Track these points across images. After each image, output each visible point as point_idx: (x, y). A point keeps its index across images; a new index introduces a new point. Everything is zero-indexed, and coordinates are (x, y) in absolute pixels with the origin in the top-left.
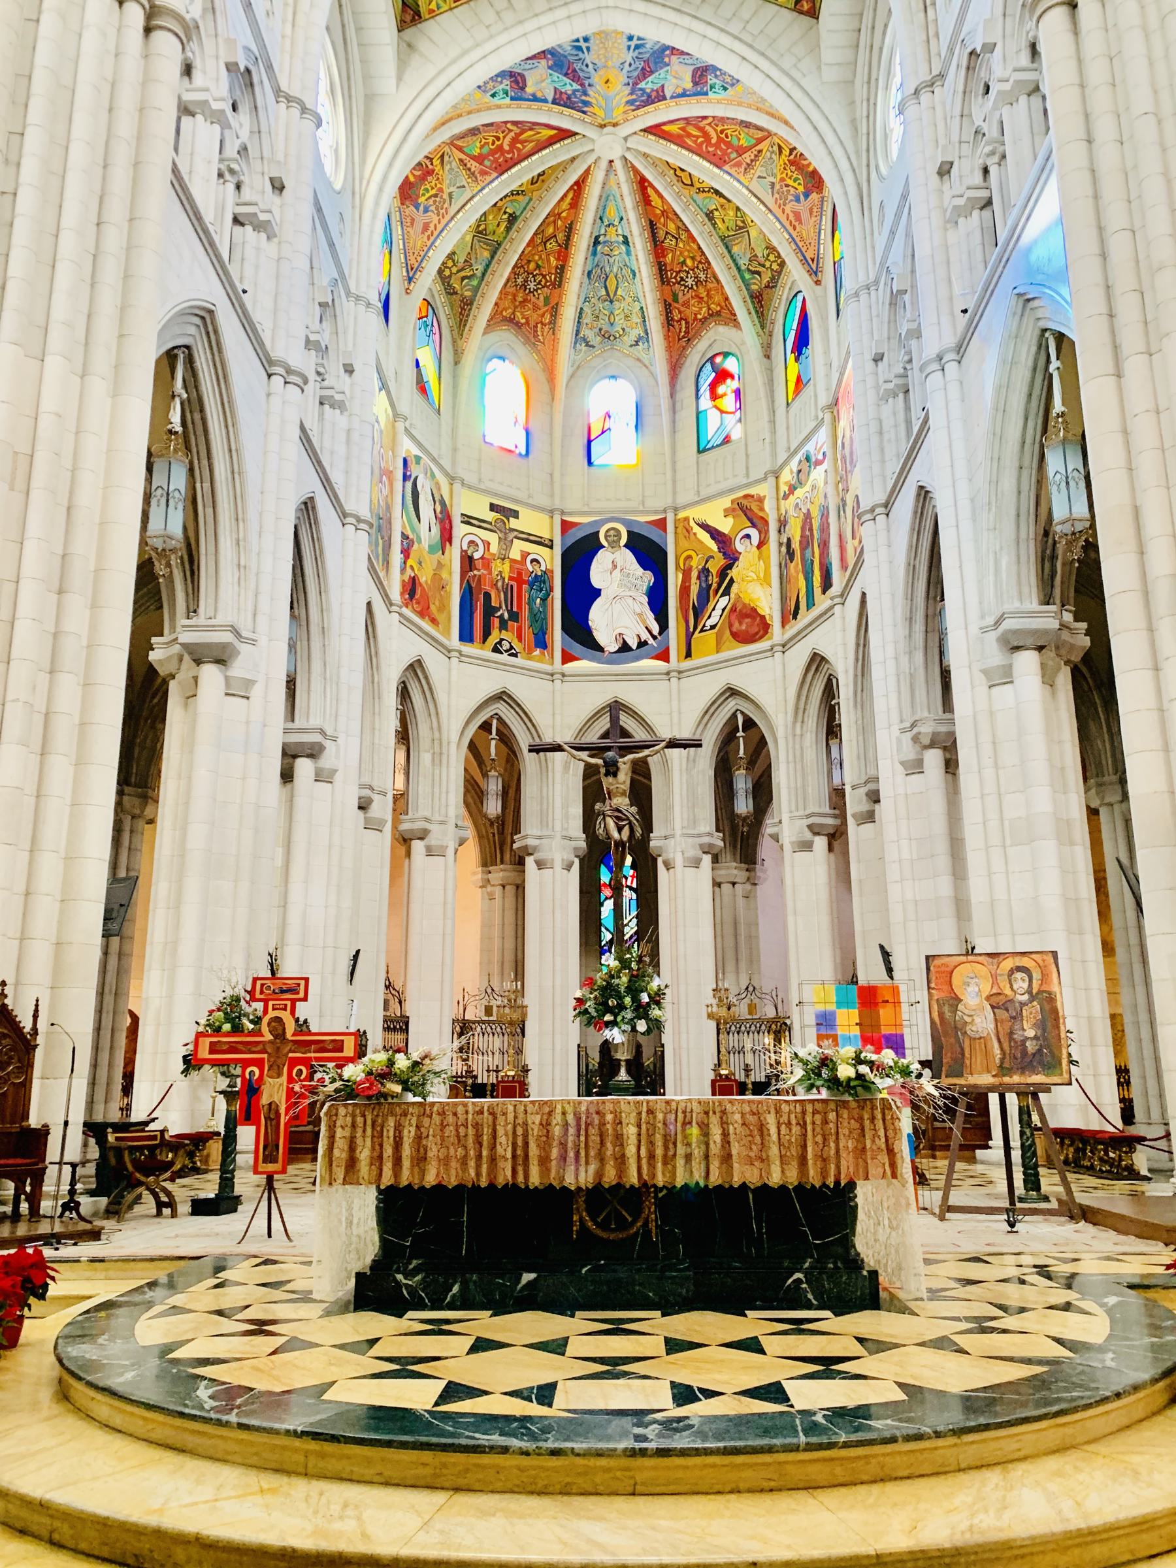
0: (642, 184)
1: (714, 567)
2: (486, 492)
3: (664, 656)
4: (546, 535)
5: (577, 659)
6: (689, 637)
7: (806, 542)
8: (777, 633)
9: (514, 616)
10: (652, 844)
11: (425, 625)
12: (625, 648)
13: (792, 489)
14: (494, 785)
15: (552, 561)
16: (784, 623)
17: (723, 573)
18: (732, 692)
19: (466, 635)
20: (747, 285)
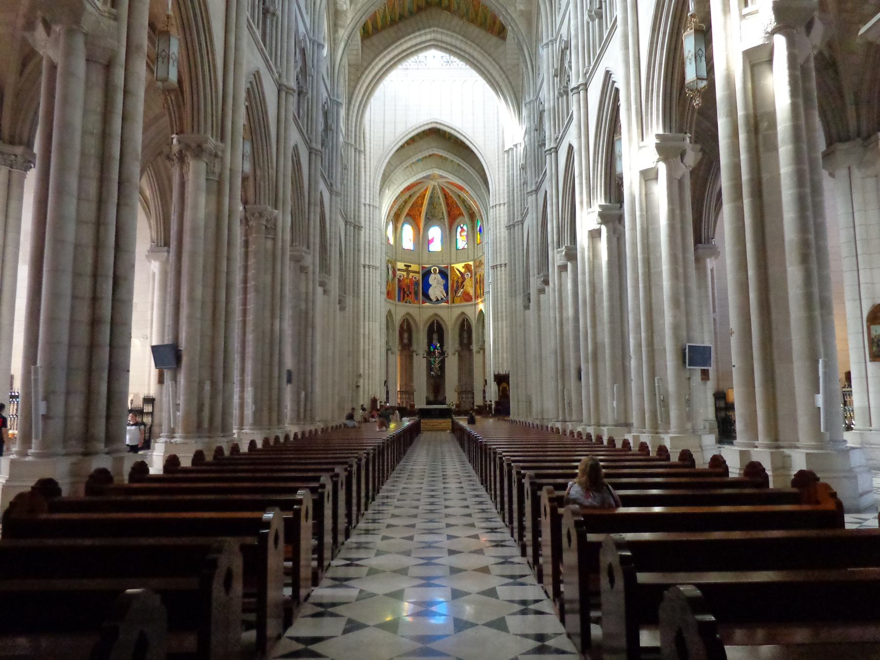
0: (443, 189)
1: (460, 281)
2: (404, 262)
3: (447, 302)
4: (417, 270)
5: (425, 303)
6: (454, 298)
7: (480, 280)
8: (473, 302)
9: (410, 293)
10: (444, 349)
11: (391, 301)
12: (438, 300)
13: (478, 266)
14: (406, 335)
15: (419, 277)
16: (475, 298)
17: (462, 282)
18: (463, 313)
19: (399, 300)
20: (468, 211)
